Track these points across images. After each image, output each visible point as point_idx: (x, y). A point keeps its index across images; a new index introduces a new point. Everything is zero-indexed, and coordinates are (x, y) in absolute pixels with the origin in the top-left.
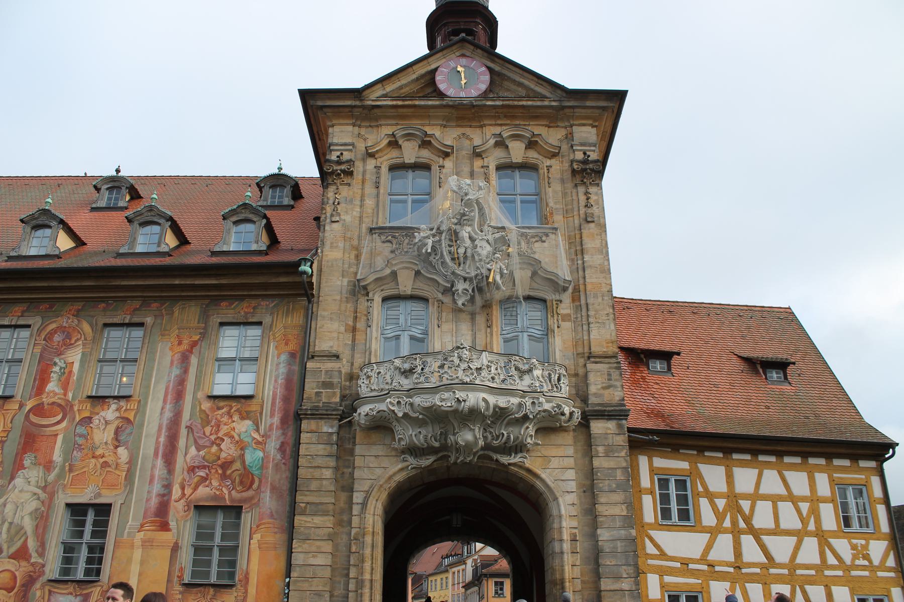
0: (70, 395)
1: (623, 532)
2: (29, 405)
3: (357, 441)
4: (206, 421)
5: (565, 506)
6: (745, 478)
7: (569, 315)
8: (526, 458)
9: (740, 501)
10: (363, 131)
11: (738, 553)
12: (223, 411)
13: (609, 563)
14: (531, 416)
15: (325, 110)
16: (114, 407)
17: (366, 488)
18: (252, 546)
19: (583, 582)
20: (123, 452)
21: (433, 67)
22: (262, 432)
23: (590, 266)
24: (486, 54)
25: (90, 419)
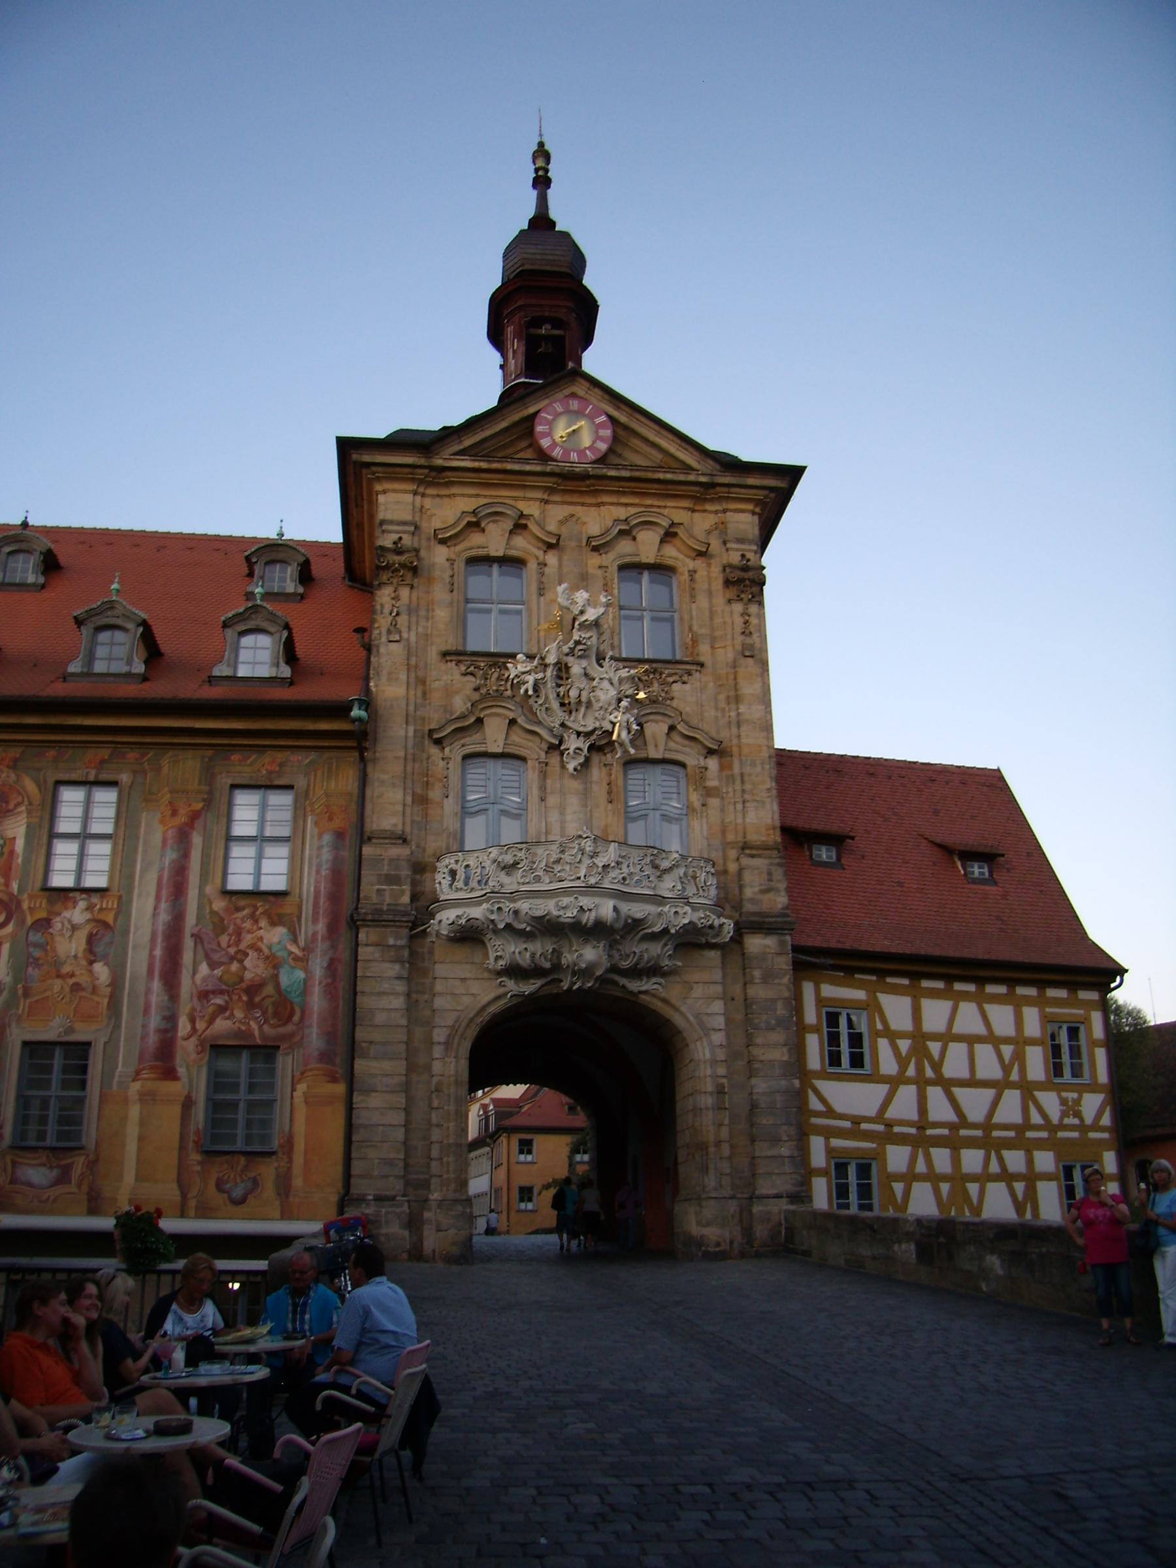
0: (15, 886)
4: (220, 927)
6: (935, 1014)
7: (716, 788)
9: (928, 1043)
10: (428, 503)
12: (245, 912)
13: (764, 1122)
14: (673, 931)
15: (374, 469)
16: (82, 905)
17: (450, 1022)
18: (296, 1100)
20: (102, 971)
21: (532, 410)
22: (302, 943)
23: (747, 721)
24: (607, 397)
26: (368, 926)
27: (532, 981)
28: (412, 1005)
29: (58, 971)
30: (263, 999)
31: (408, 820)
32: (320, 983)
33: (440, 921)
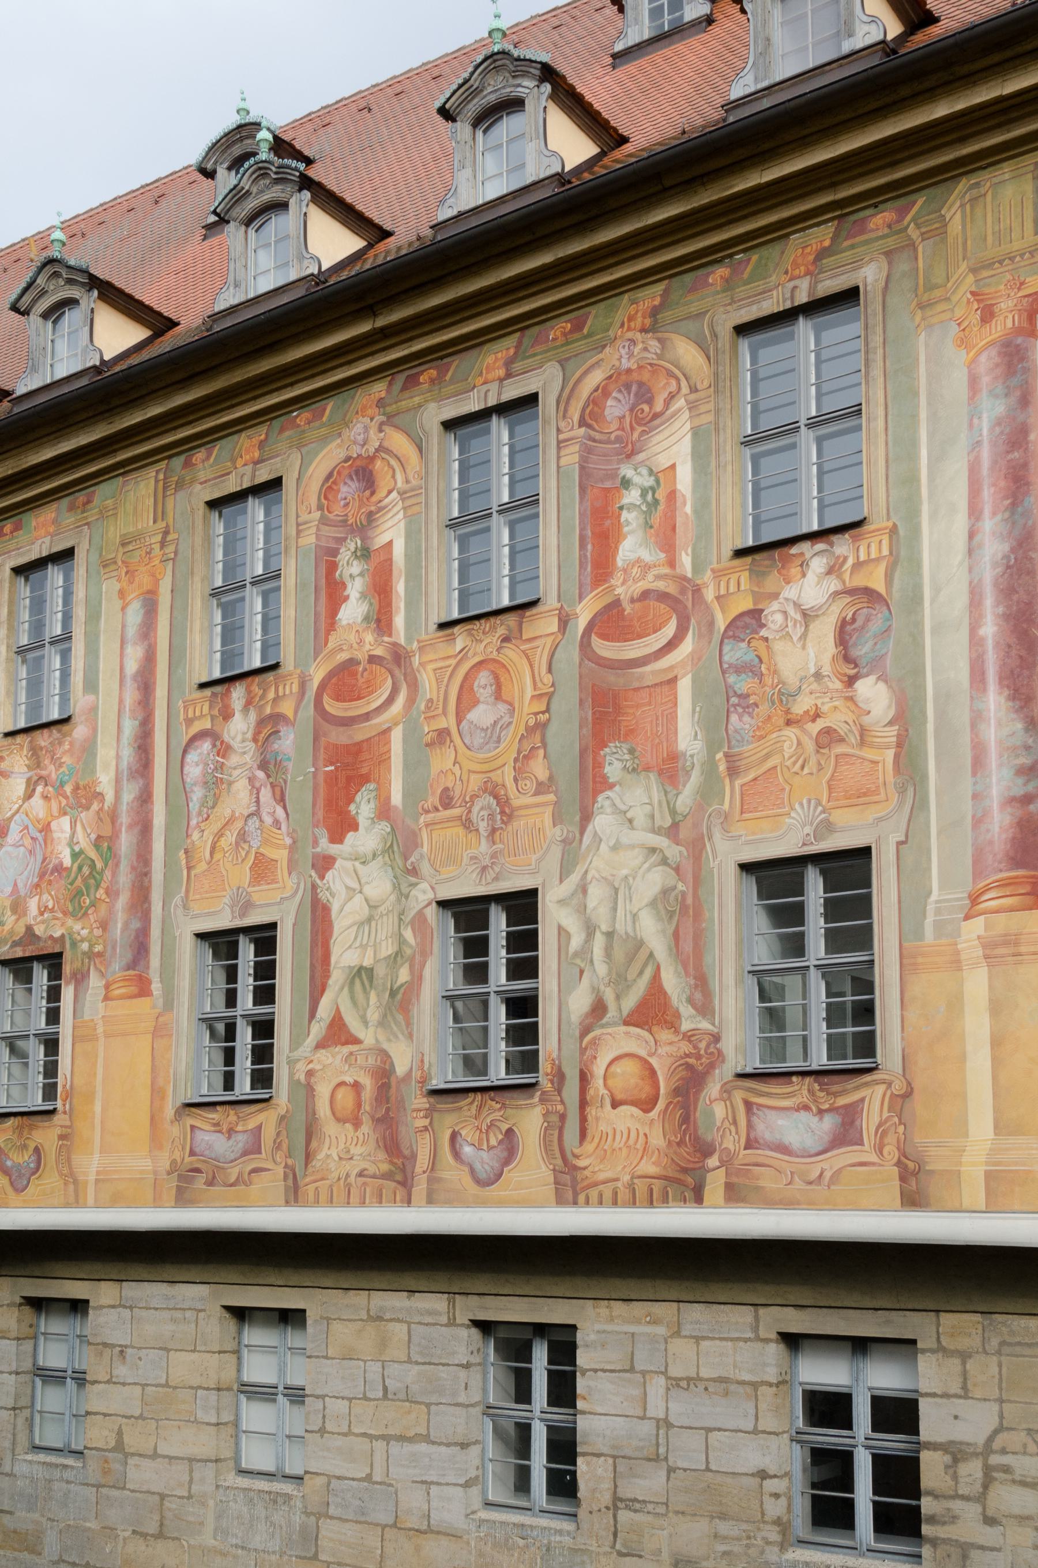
2: (584, 614)
25: (755, 616)
29: (788, 712)
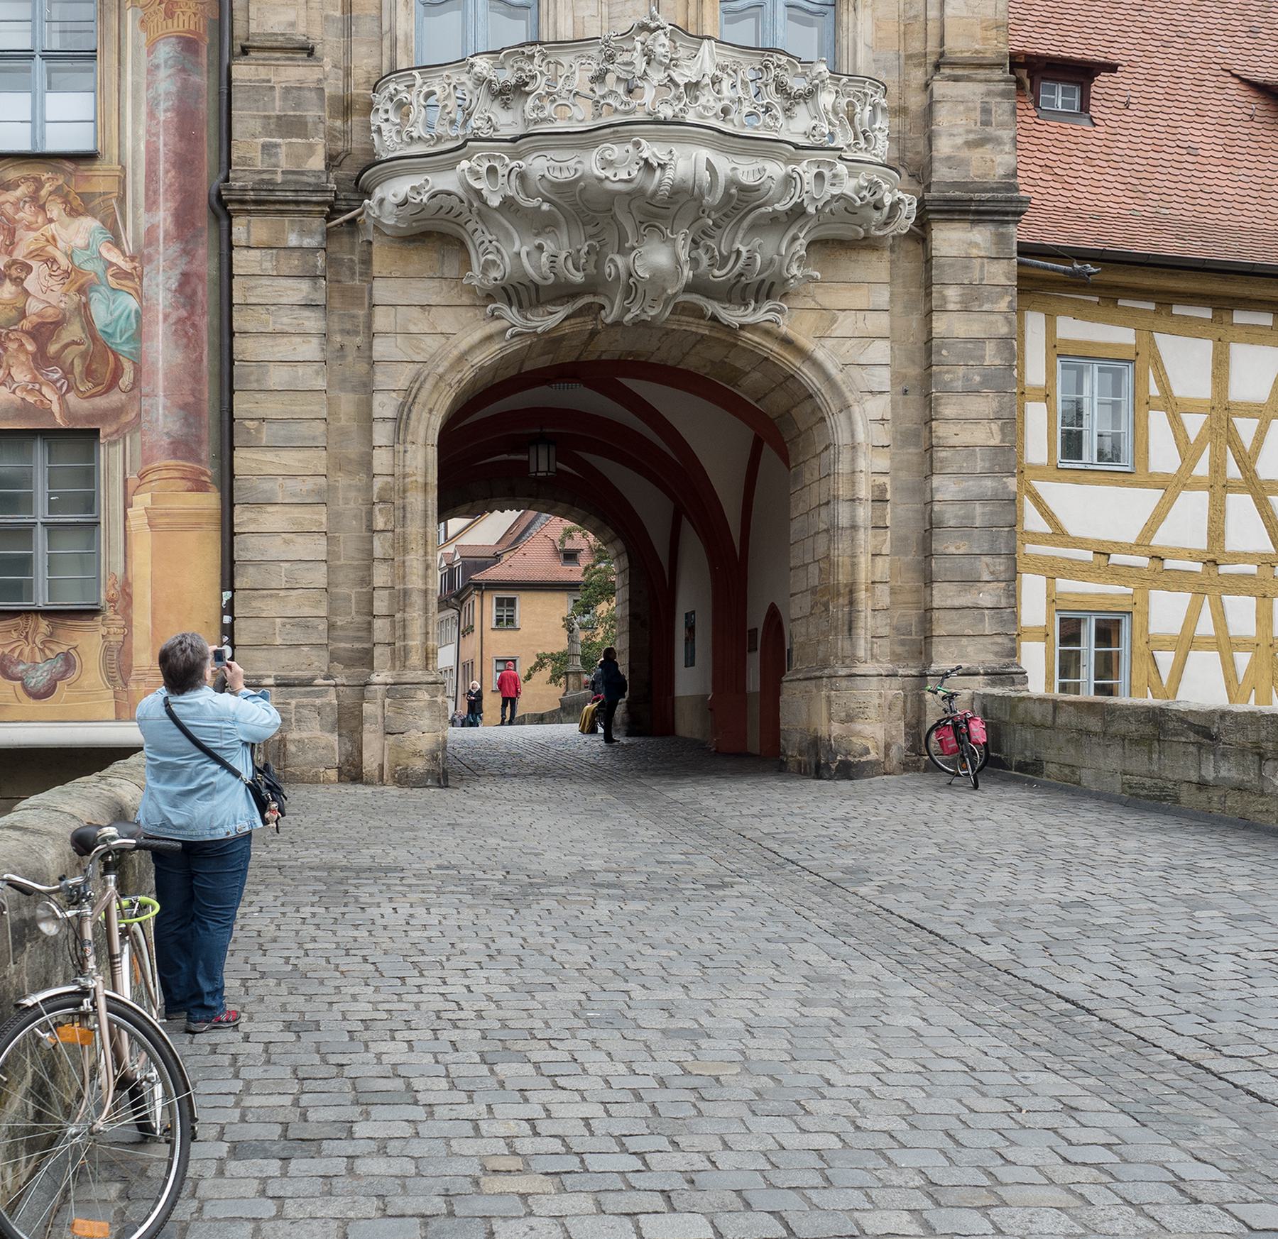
1: (989, 483)
3: (376, 268)
5: (865, 426)
8: (781, 312)
11: (1216, 532)
17: (403, 383)
19: (893, 592)
22: (129, 247)
26: (249, 212)
27: (550, 308)
28: (333, 356)
30: (66, 346)
31: (316, 15)
32: (166, 317)
33: (382, 201)
